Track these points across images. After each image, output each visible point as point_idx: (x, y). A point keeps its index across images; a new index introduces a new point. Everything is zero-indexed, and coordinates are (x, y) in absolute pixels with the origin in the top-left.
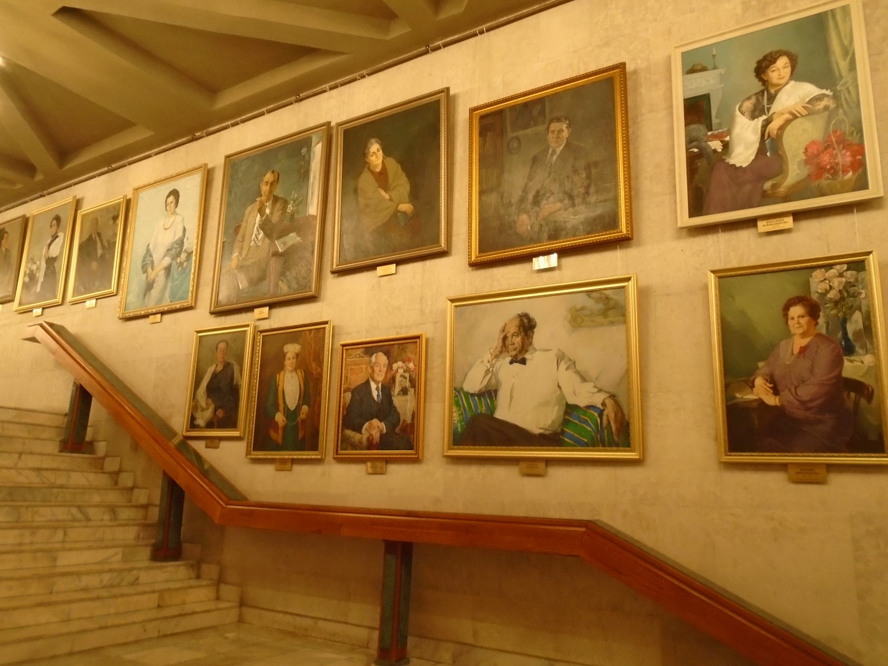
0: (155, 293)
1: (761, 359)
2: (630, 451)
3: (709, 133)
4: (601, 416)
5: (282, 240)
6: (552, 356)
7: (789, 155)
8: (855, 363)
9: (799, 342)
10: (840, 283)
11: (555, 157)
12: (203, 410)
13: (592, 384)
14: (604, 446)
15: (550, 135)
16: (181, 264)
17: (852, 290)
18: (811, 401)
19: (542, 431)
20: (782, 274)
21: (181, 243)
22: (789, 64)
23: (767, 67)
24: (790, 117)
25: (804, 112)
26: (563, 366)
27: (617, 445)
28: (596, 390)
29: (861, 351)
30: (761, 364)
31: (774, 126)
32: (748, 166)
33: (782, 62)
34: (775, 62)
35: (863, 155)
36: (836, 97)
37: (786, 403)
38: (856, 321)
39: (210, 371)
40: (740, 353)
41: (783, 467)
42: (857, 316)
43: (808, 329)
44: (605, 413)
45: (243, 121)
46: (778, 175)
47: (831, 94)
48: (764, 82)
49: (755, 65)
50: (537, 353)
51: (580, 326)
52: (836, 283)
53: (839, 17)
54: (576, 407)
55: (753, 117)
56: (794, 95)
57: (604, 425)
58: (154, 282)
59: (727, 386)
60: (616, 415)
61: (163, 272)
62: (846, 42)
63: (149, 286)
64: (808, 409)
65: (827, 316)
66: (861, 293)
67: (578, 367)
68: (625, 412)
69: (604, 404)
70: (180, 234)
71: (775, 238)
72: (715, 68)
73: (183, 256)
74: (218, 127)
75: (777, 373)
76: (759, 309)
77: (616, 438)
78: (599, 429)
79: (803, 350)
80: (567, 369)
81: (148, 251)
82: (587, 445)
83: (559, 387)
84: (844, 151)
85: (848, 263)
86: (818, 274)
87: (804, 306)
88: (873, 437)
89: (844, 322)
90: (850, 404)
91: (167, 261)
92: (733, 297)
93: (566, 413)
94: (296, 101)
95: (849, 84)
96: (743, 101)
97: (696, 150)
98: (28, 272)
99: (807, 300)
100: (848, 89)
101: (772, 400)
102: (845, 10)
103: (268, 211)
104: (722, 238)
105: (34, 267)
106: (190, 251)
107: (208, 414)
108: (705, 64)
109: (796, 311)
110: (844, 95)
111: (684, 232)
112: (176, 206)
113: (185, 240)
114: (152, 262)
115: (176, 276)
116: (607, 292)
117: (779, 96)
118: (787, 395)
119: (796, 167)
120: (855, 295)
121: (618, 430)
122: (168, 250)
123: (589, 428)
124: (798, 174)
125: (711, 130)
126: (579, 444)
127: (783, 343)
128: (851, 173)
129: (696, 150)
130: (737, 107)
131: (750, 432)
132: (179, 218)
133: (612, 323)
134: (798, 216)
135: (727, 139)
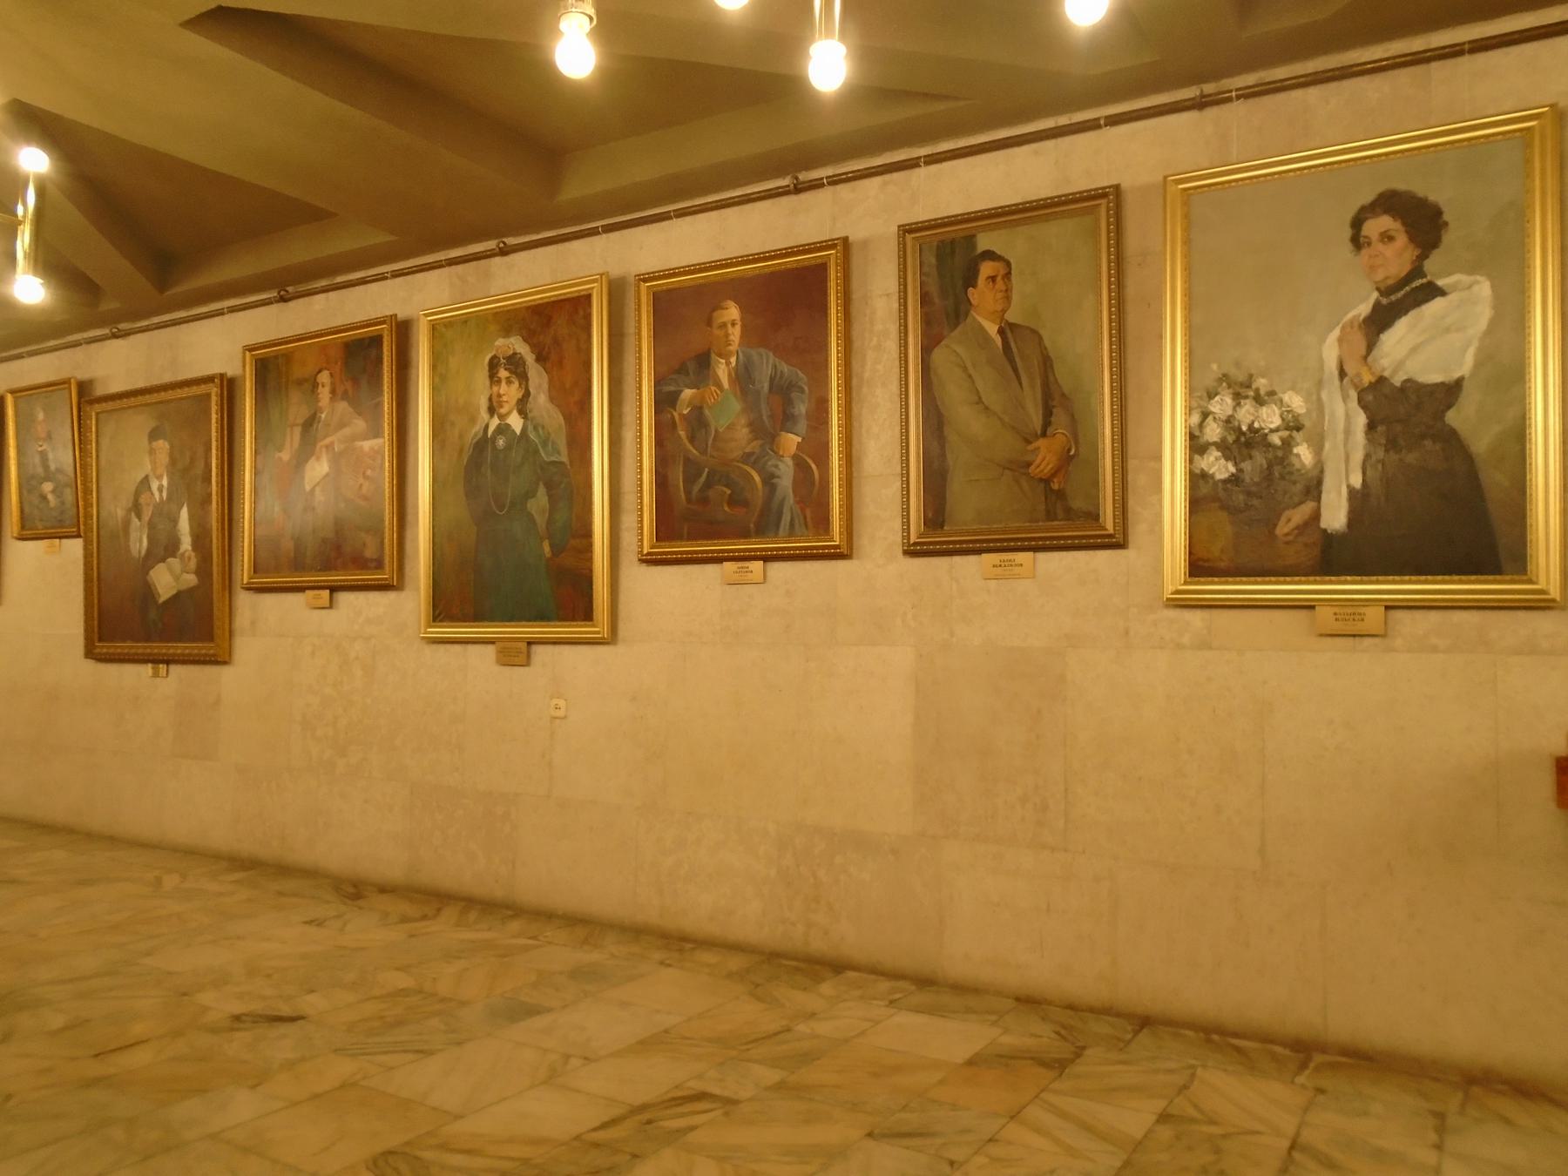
98: (1213, 432)
105: (1270, 418)
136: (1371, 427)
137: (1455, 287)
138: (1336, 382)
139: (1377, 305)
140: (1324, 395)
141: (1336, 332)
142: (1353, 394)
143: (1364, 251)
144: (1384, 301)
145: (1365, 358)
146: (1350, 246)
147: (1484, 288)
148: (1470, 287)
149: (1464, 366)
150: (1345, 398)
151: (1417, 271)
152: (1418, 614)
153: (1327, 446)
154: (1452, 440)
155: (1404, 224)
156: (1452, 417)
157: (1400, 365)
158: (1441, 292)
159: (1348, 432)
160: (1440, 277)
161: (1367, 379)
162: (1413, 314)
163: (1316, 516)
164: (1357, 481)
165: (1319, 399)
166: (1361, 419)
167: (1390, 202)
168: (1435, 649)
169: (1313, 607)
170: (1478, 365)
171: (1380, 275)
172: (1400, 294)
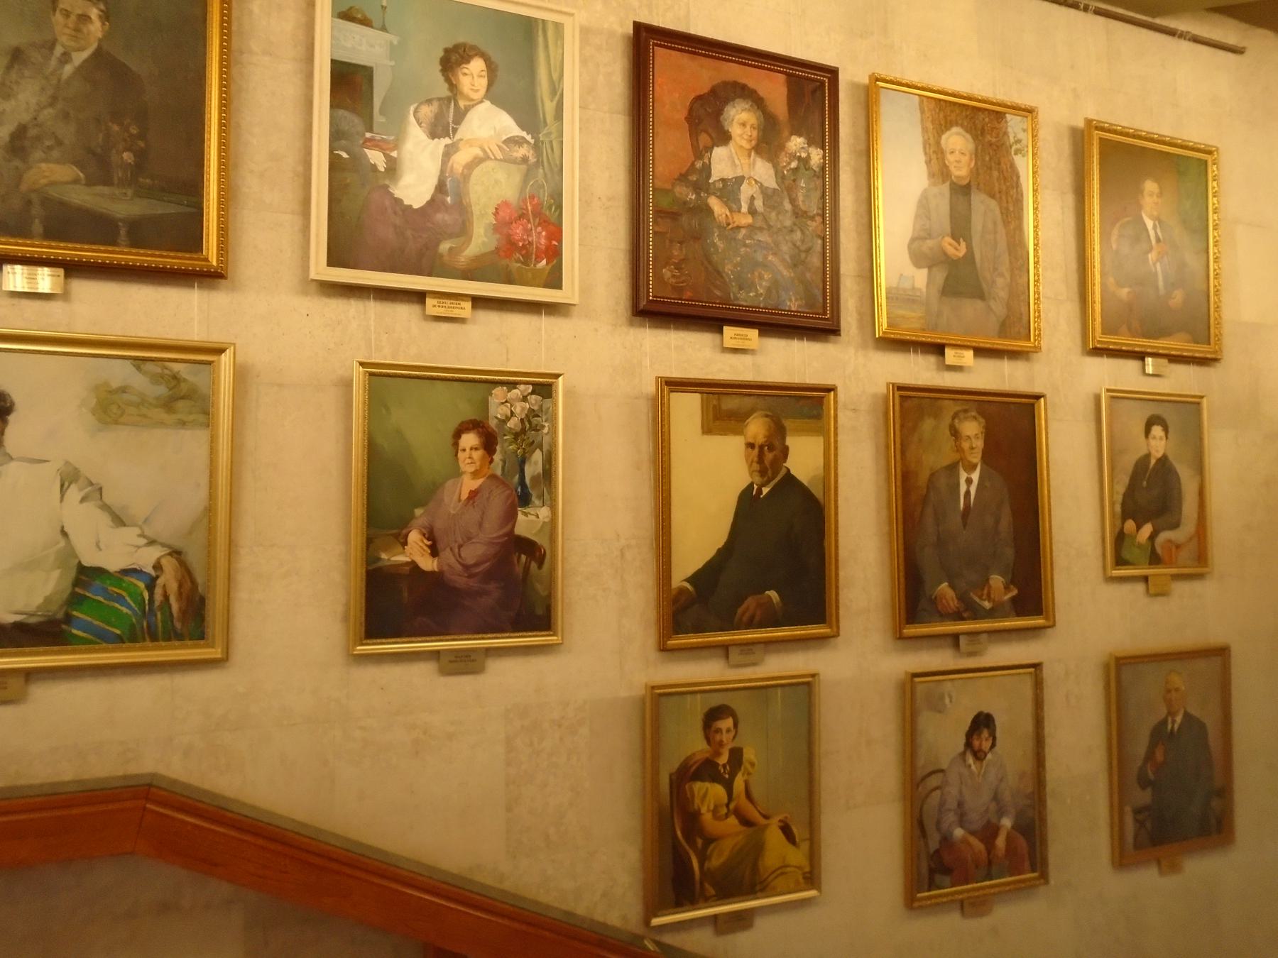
1: (422, 504)
2: (208, 646)
3: (368, 135)
4: (151, 586)
6: (49, 474)
7: (476, 210)
8: (532, 518)
9: (469, 484)
10: (523, 409)
11: (68, 69)
13: (137, 531)
14: (154, 638)
15: (58, 17)
17: (535, 421)
18: (476, 565)
19: (18, 618)
20: (455, 383)
22: (485, 73)
23: (459, 64)
24: (481, 154)
25: (500, 156)
26: (74, 493)
27: (179, 637)
28: (143, 541)
29: (537, 502)
30: (418, 512)
31: (460, 159)
32: (422, 208)
33: (477, 65)
34: (468, 62)
35: (560, 241)
36: (537, 147)
37: (445, 568)
38: (536, 463)
40: (389, 492)
41: (436, 655)
42: (537, 456)
43: (481, 466)
44: (160, 582)
46: (458, 236)
47: (532, 141)
48: (453, 87)
49: (441, 54)
50: (13, 464)
51: (116, 422)
52: (519, 408)
53: (550, 33)
54: (99, 572)
55: (433, 135)
56: (488, 124)
57: (157, 603)
59: (369, 541)
60: (180, 586)
62: (555, 76)
64: (471, 576)
65: (504, 452)
66: (543, 427)
67: (108, 498)
68: (200, 580)
69: (158, 566)
71: (445, 327)
72: (384, 29)
75: (439, 525)
76: (422, 429)
77: (178, 625)
78: (147, 611)
79: (473, 494)
80: (83, 500)
82: (119, 639)
83: (64, 534)
84: (539, 229)
85: (534, 384)
86: (499, 392)
87: (480, 435)
88: (540, 611)
89: (523, 462)
90: (519, 570)
92: (387, 409)
93: (77, 583)
95: (553, 136)
96: (421, 103)
97: (345, 155)
99: (483, 427)
100: (551, 142)
101: (428, 564)
102: (558, 27)
104: (373, 308)
108: (369, 15)
109: (469, 440)
110: (546, 148)
111: (313, 287)
116: (176, 367)
117: (469, 116)
118: (447, 556)
119: (482, 231)
120: (537, 429)
121: (183, 612)
123: (125, 610)
124: (484, 243)
125: (371, 130)
126: (103, 638)
127: (449, 483)
128: (544, 262)
129: (345, 155)
130: (412, 108)
131: (395, 605)
133: (183, 424)
134: (479, 302)
135: (394, 154)
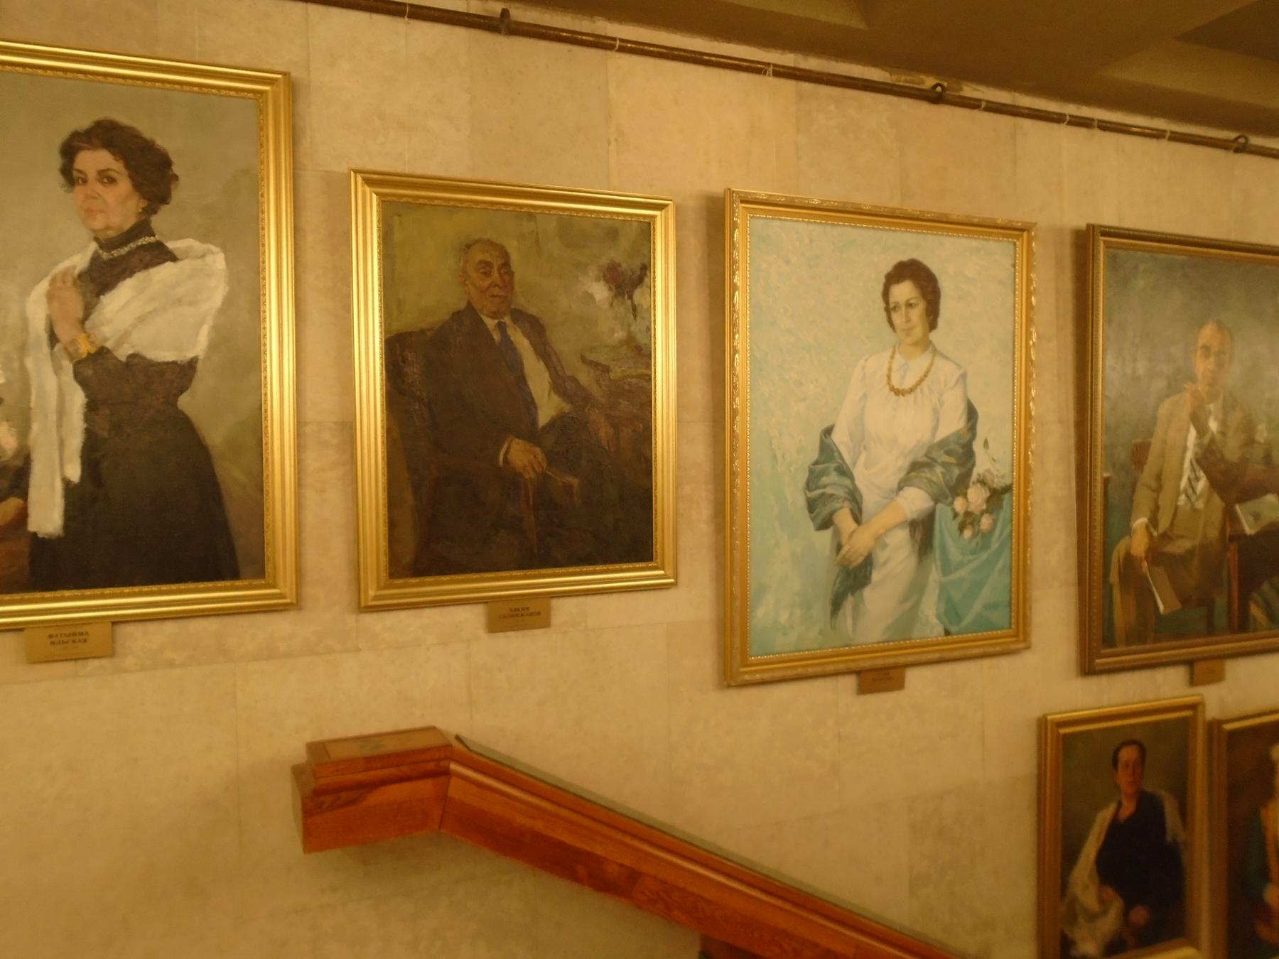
0: (879, 604)
5: (1251, 505)
12: (1092, 917)
16: (968, 520)
21: (962, 451)
39: (1103, 818)
45: (1105, 126)
58: (868, 562)
61: (902, 535)
63: (854, 577)
70: (953, 423)
73: (976, 497)
74: (1003, 97)
81: (827, 450)
91: (915, 501)
94: (1237, 151)
103: (1213, 425)
106: (998, 483)
107: (1109, 923)
112: (932, 325)
113: (977, 446)
114: (854, 498)
115: (955, 555)
122: (915, 467)
132: (945, 371)
136: (92, 408)
137: (187, 254)
138: (46, 348)
139: (95, 259)
140: (29, 363)
141: (44, 286)
142: (68, 366)
143: (78, 189)
144: (105, 256)
145: (83, 321)
146: (60, 179)
147: (218, 261)
148: (203, 256)
149: (198, 347)
150: (57, 370)
151: (142, 228)
152: (152, 627)
153: (35, 427)
154: (185, 425)
155: (127, 166)
156: (184, 402)
157: (124, 337)
158: (174, 259)
159: (61, 411)
160: (171, 239)
161: (85, 348)
162: (139, 276)
163: (23, 516)
164: (74, 472)
165: (23, 368)
166: (78, 399)
167: (106, 134)
168: (171, 664)
169: (21, 630)
170: (213, 346)
171: (99, 223)
172: (124, 251)
